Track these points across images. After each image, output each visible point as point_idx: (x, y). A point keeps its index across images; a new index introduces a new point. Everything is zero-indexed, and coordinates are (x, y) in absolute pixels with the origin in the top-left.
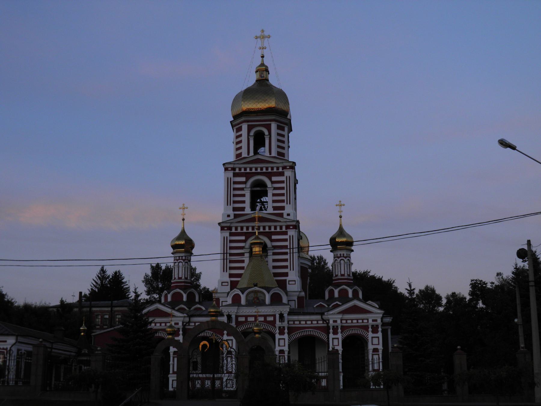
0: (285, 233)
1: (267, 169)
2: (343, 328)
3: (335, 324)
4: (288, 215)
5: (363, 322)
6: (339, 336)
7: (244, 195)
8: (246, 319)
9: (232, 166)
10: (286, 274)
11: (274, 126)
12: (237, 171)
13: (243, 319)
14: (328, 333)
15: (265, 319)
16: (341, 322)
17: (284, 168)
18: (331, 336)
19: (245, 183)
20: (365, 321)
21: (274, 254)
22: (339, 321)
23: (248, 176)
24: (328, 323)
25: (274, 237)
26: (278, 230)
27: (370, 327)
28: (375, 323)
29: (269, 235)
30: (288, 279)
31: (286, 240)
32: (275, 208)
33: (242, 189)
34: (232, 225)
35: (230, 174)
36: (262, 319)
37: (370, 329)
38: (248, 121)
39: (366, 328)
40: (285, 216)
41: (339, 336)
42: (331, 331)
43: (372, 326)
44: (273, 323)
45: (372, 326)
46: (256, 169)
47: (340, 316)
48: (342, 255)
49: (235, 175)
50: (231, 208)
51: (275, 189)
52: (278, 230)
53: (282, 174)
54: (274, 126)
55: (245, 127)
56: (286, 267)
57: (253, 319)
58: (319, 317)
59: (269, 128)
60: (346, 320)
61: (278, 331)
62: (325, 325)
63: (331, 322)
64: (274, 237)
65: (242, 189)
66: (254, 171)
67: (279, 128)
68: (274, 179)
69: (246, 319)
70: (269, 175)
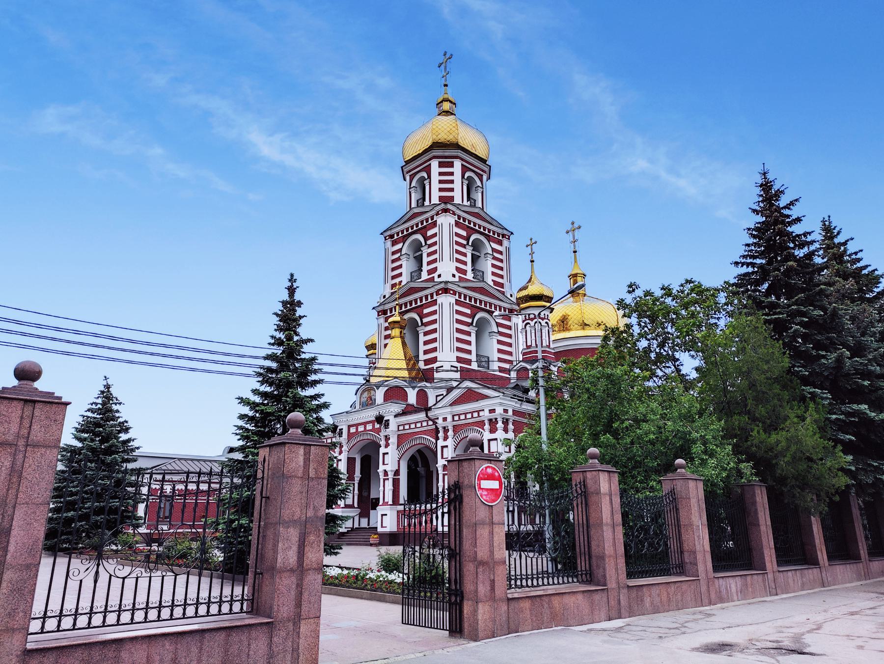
0: (434, 303)
1: (422, 223)
3: (445, 424)
4: (439, 276)
5: (479, 416)
7: (400, 266)
8: (357, 429)
9: (389, 233)
10: (434, 360)
11: (435, 164)
12: (396, 237)
13: (353, 430)
14: (437, 439)
15: (373, 426)
17: (437, 214)
18: (441, 443)
19: (400, 250)
21: (426, 334)
22: (449, 419)
23: (404, 239)
24: (435, 423)
25: (426, 311)
26: (429, 300)
27: (487, 422)
28: (492, 416)
29: (419, 310)
30: (435, 366)
31: (435, 312)
32: (430, 272)
33: (398, 259)
34: (387, 307)
35: (389, 242)
36: (369, 427)
37: (487, 427)
38: (410, 171)
39: (481, 424)
40: (436, 279)
42: (441, 435)
43: (490, 420)
44: (378, 431)
45: (490, 420)
46: (412, 228)
47: (449, 409)
49: (394, 243)
50: (388, 286)
51: (430, 246)
52: (429, 300)
53: (434, 224)
54: (435, 164)
55: (408, 178)
56: (435, 350)
57: (361, 428)
59: (428, 170)
61: (383, 443)
63: (440, 421)
64: (426, 311)
65: (398, 259)
66: (410, 231)
67: (441, 165)
68: (430, 233)
69: (357, 429)
70: (423, 231)
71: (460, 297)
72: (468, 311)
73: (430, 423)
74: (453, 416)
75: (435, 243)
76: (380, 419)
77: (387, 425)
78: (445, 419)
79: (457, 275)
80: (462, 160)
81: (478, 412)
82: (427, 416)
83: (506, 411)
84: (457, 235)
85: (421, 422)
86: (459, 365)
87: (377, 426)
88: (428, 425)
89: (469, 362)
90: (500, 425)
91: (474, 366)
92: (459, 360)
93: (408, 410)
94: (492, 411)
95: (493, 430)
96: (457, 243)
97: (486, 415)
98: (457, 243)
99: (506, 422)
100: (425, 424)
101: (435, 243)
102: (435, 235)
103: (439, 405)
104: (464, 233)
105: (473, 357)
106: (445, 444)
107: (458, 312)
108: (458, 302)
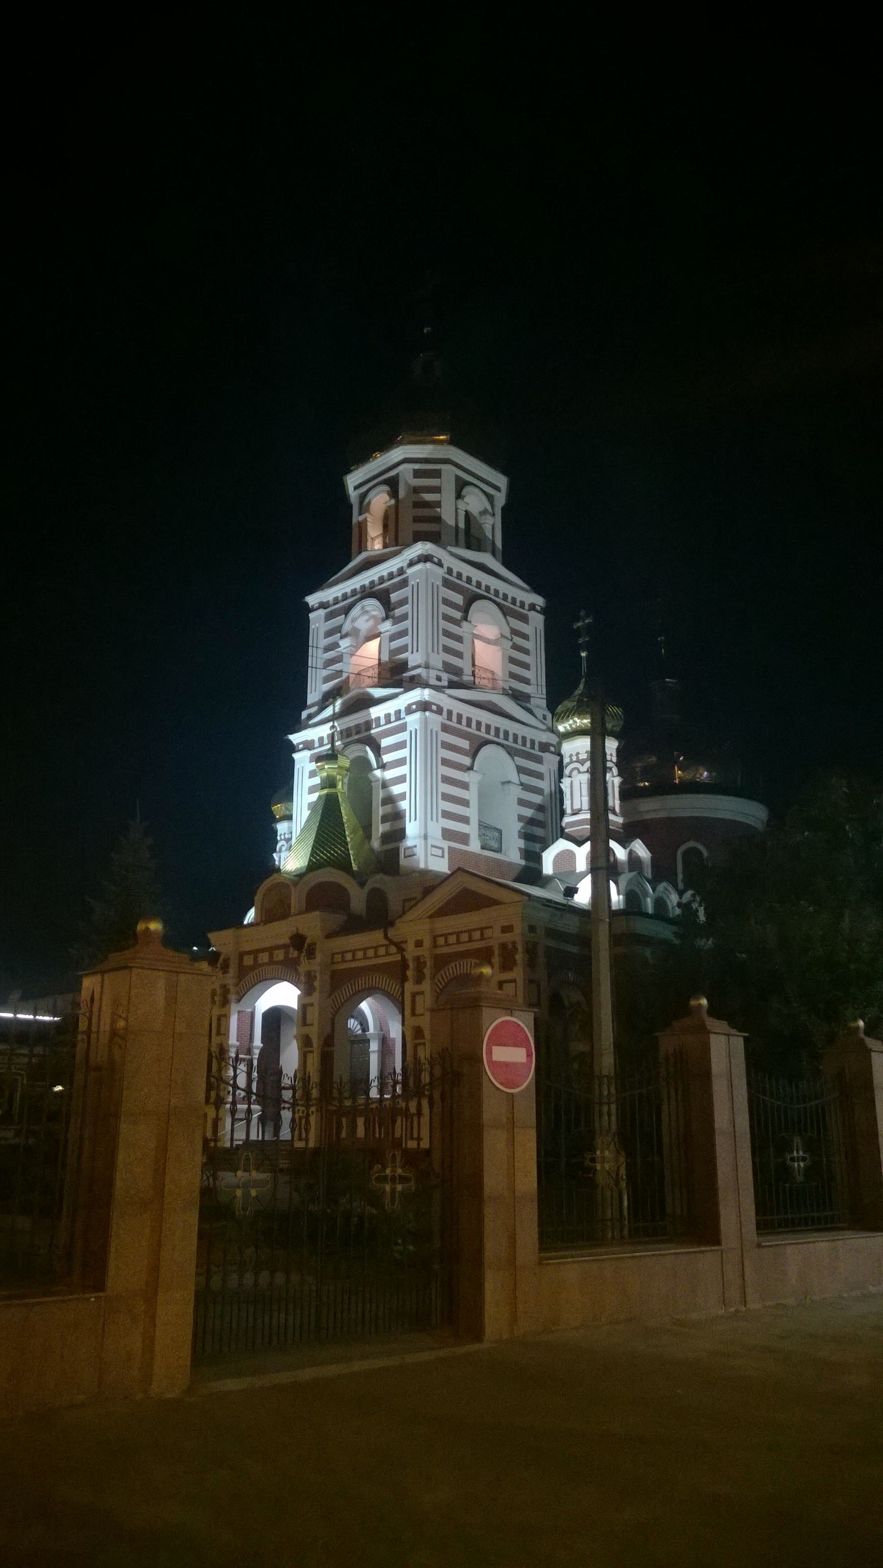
2: (441, 962)
3: (419, 952)
5: (482, 938)
6: (426, 986)
8: (256, 959)
14: (404, 979)
15: (287, 953)
16: (435, 945)
20: (488, 933)
22: (427, 943)
27: (496, 951)
28: (508, 937)
36: (280, 955)
41: (426, 986)
42: (410, 973)
45: (503, 946)
48: (574, 758)
53: (404, 583)
58: (377, 937)
60: (446, 936)
62: (398, 957)
63: (410, 947)
69: (256, 959)
71: (449, 718)
72: (465, 744)
73: (393, 949)
74: (435, 938)
75: (404, 617)
76: (298, 941)
77: (311, 954)
78: (419, 944)
79: (445, 677)
80: (457, 465)
81: (482, 929)
82: (386, 937)
83: (532, 929)
84: (446, 602)
85: (376, 948)
86: (446, 844)
87: (294, 954)
88: (388, 954)
89: (464, 838)
90: (519, 957)
91: (474, 846)
92: (447, 834)
93: (354, 925)
94: (507, 929)
95: (507, 964)
96: (446, 618)
97: (496, 938)
98: (446, 618)
99: (531, 951)
100: (382, 951)
101: (404, 617)
102: (403, 602)
103: (409, 916)
104: (458, 599)
105: (472, 830)
106: (417, 988)
107: (446, 746)
108: (445, 728)
